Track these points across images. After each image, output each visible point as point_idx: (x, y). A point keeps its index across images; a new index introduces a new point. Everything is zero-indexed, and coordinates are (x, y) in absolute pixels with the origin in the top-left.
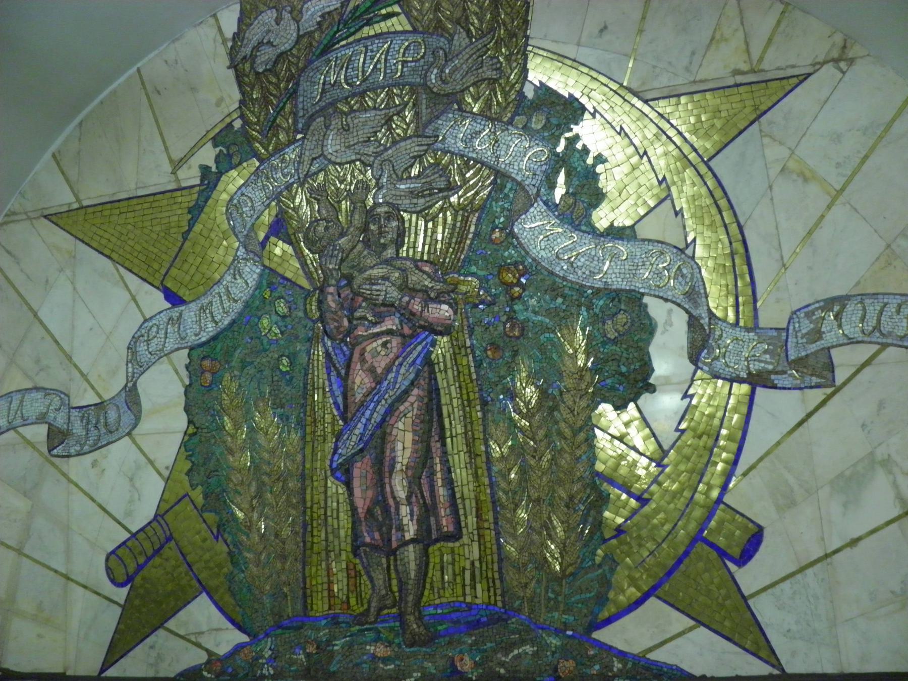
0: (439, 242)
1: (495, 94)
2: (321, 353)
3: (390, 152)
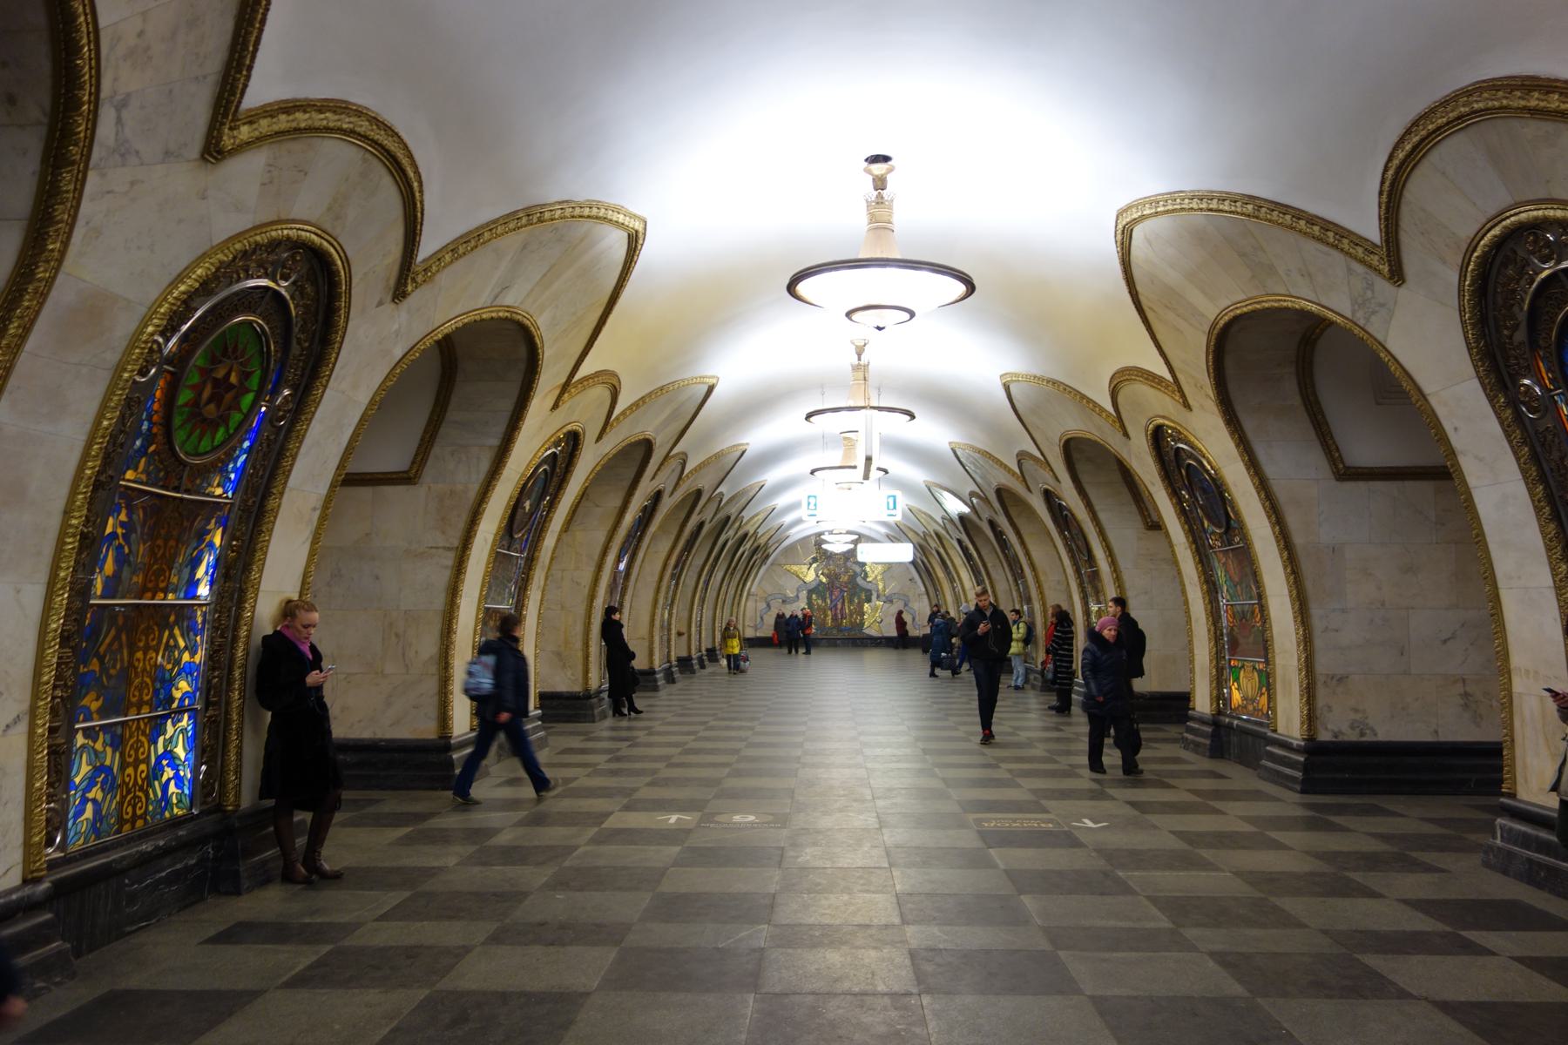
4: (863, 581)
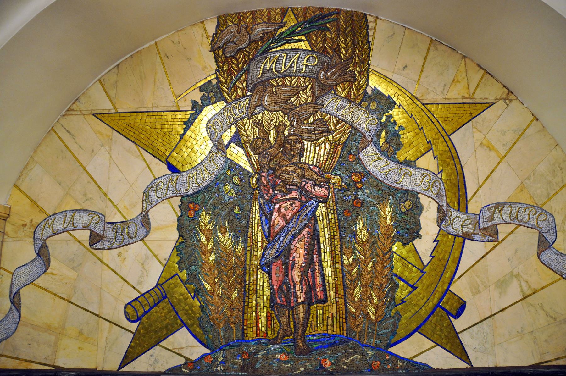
0: (322, 157)
1: (353, 89)
2: (257, 206)
3: (298, 109)
4: (382, 162)
